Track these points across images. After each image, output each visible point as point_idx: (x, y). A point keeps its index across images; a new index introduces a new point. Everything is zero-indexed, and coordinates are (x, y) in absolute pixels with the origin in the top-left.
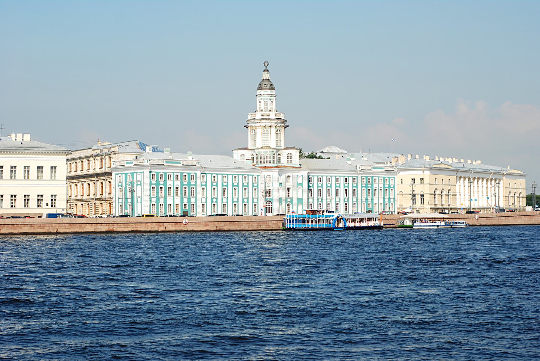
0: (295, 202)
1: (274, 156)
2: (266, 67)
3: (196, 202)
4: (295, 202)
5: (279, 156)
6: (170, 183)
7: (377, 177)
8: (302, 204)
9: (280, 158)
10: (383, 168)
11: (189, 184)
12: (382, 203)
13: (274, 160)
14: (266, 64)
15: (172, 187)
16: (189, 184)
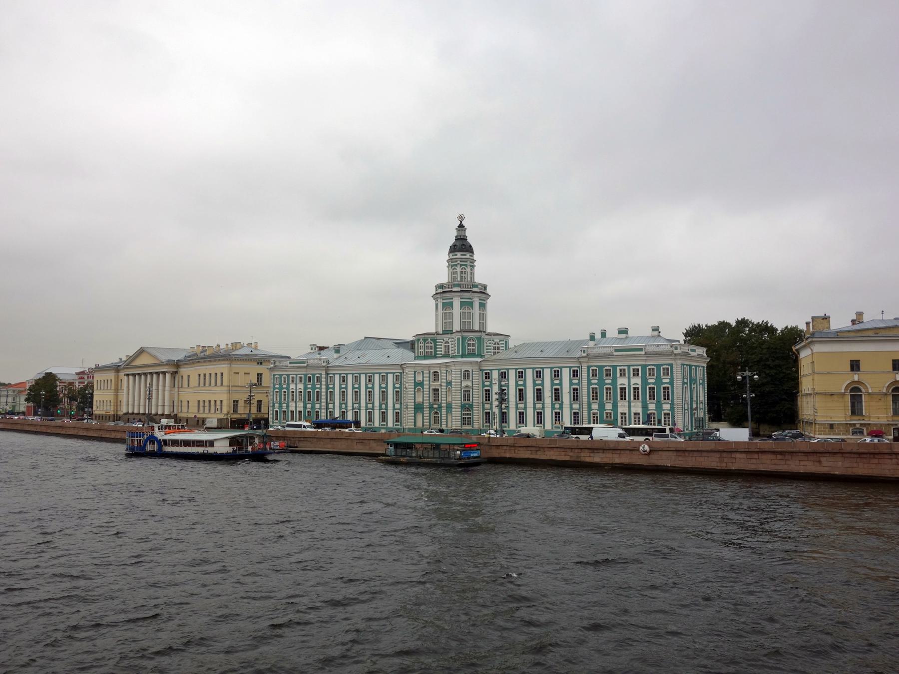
0: (444, 410)
1: (421, 345)
2: (461, 222)
3: (320, 408)
4: (444, 410)
5: (447, 344)
6: (292, 386)
7: (624, 366)
8: (451, 412)
9: (449, 346)
10: (641, 350)
11: (314, 387)
12: (640, 410)
13: (421, 350)
14: (461, 218)
15: (294, 390)
16: (314, 387)
